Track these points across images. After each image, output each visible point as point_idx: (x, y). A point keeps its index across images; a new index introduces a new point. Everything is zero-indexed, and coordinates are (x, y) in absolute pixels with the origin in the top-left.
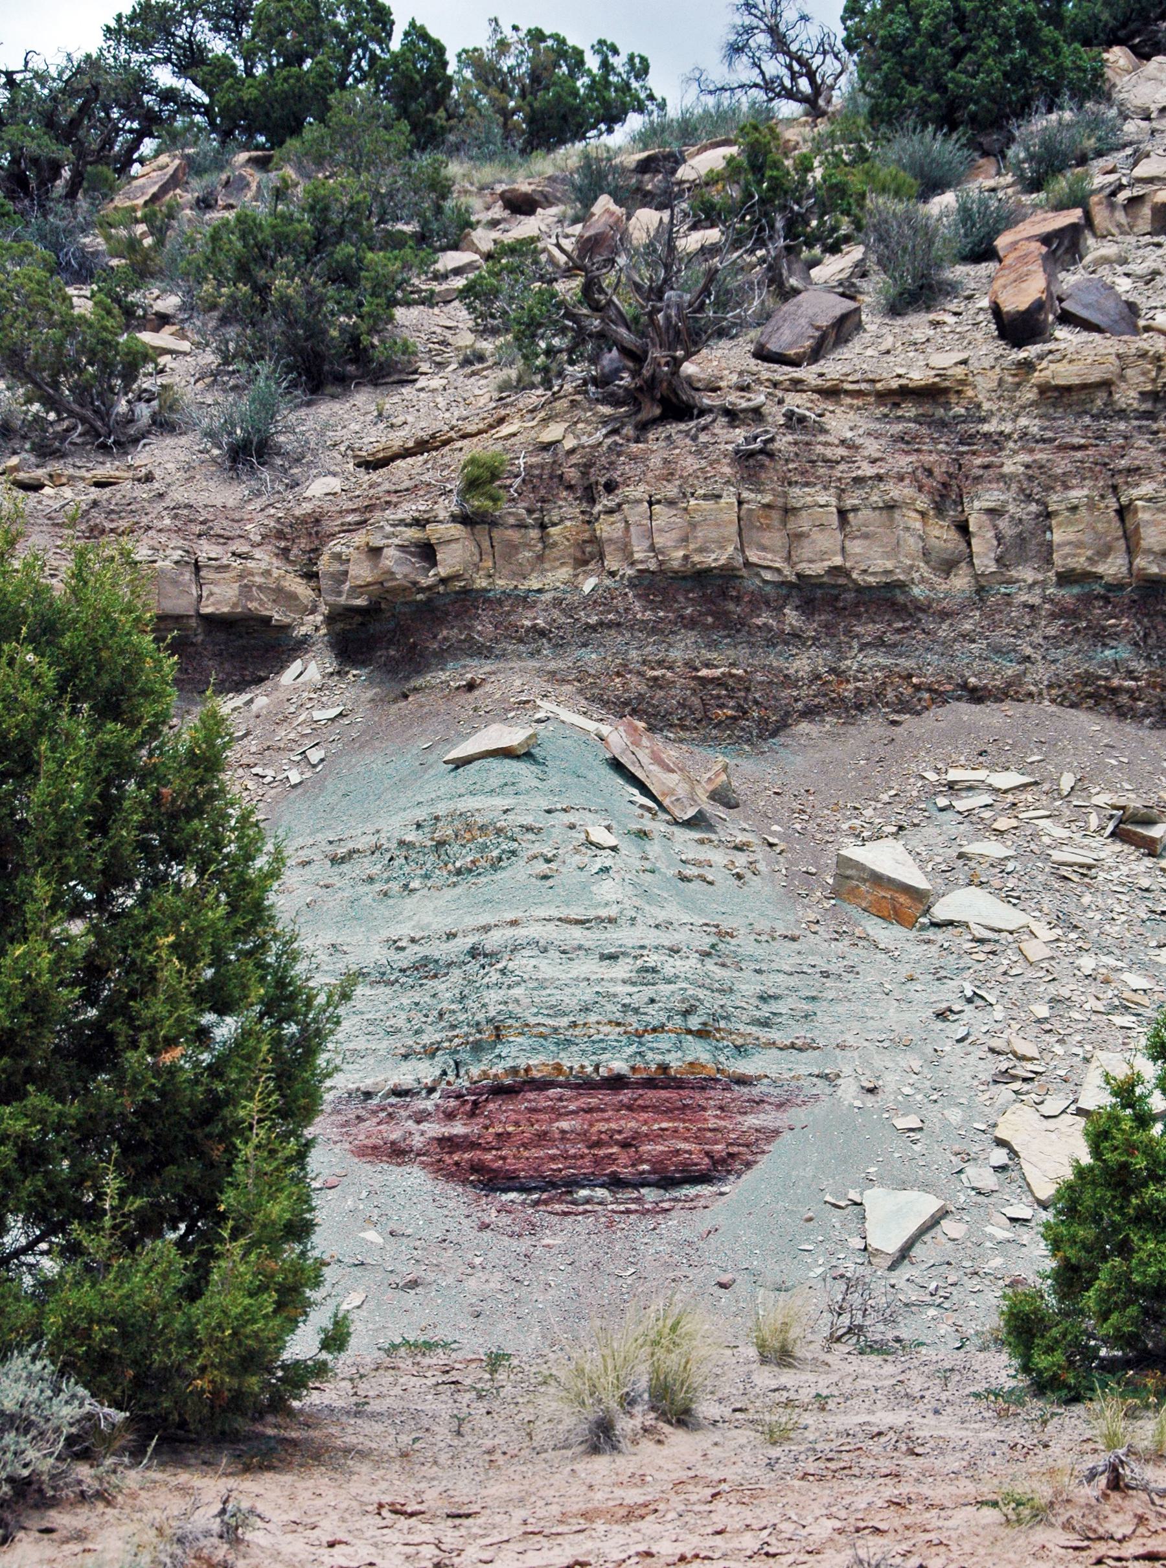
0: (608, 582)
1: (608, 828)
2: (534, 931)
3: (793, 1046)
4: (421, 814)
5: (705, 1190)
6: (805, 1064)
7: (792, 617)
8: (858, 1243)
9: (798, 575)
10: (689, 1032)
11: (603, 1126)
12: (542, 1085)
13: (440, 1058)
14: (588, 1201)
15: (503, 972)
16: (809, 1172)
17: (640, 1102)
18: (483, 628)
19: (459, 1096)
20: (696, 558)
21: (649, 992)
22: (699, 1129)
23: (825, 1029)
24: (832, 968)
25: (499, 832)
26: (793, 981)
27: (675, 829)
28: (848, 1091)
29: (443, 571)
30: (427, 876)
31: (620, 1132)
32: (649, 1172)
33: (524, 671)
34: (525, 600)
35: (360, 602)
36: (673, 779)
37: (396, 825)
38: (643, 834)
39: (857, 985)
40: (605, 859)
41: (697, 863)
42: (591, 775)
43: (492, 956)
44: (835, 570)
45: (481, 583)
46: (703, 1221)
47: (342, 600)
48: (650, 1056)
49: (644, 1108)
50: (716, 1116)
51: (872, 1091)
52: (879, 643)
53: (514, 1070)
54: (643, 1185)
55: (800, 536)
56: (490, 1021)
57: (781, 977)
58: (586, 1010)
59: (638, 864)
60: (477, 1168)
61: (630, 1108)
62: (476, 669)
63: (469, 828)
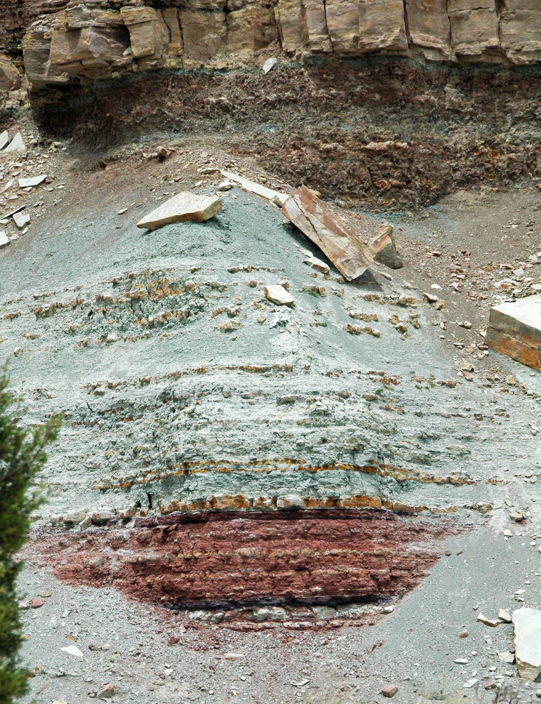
0: (286, 62)
1: (285, 286)
2: (219, 378)
3: (449, 481)
4: (118, 273)
5: (372, 609)
6: (460, 497)
7: (452, 94)
8: (507, 657)
9: (458, 55)
10: (357, 468)
11: (280, 552)
12: (227, 515)
13: (135, 491)
14: (266, 618)
15: (191, 414)
16: (464, 593)
17: (313, 530)
18: (173, 104)
19: (151, 525)
20: (365, 40)
21: (321, 432)
22: (366, 555)
23: (479, 466)
24: (485, 412)
25: (188, 289)
26: (450, 423)
27: (345, 287)
28: (499, 520)
29: (136, 51)
30: (123, 329)
31: (295, 557)
32: (321, 593)
33: (209, 143)
34: (210, 79)
35: (61, 79)
36: (343, 242)
37: (95, 282)
38: (316, 292)
39: (507, 427)
40: (282, 314)
41: (364, 318)
42: (270, 239)
43: (182, 401)
44: (491, 50)
45: (173, 63)
46: (369, 636)
47: (44, 77)
48: (322, 490)
49: (316, 536)
50: (381, 544)
51: (520, 521)
52: (531, 117)
53: (201, 502)
54: (316, 605)
55: (460, 19)
56: (179, 458)
57: (438, 420)
58: (265, 448)
59: (311, 319)
60: (167, 589)
61: (304, 536)
62: (167, 141)
63: (160, 286)
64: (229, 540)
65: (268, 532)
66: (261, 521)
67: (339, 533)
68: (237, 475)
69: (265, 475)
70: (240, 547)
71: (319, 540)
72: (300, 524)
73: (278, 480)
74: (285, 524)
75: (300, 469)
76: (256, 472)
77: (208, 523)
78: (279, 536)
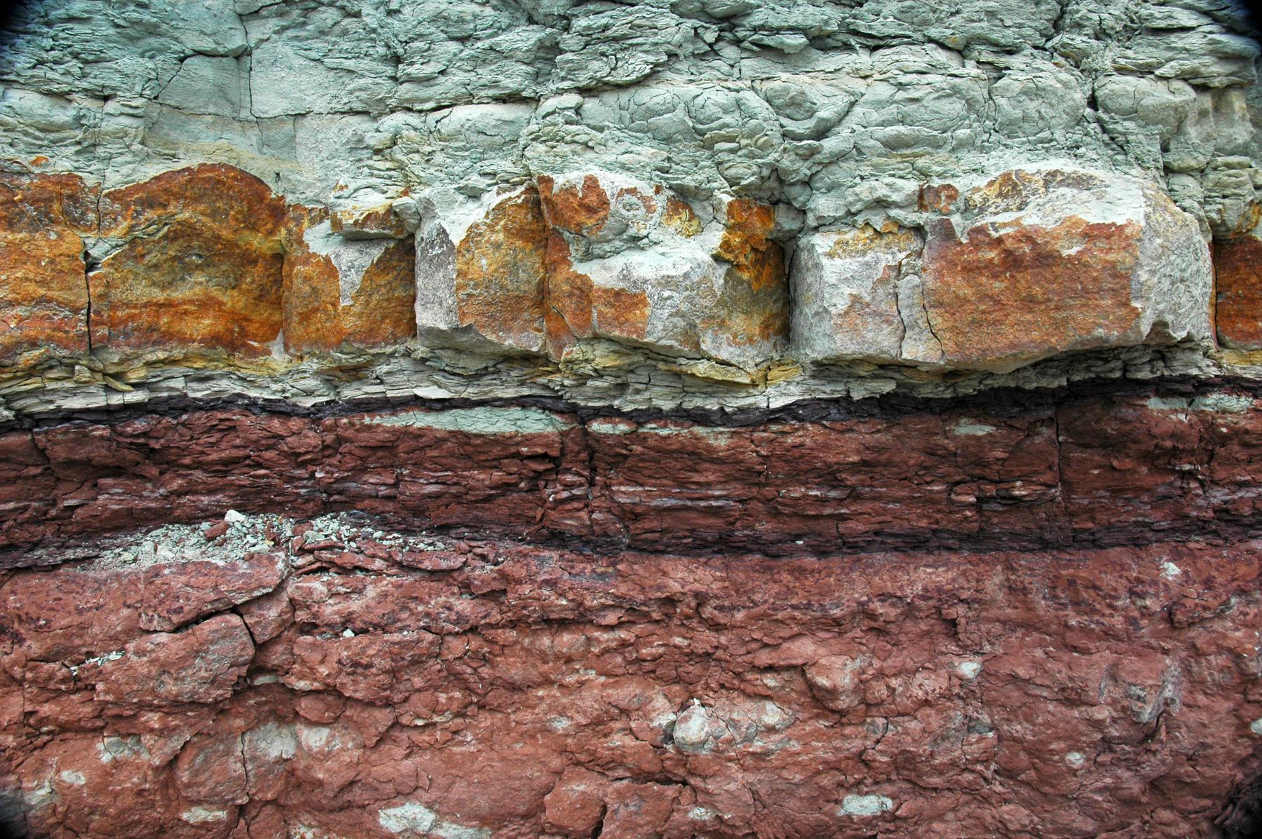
66: (548, 575)
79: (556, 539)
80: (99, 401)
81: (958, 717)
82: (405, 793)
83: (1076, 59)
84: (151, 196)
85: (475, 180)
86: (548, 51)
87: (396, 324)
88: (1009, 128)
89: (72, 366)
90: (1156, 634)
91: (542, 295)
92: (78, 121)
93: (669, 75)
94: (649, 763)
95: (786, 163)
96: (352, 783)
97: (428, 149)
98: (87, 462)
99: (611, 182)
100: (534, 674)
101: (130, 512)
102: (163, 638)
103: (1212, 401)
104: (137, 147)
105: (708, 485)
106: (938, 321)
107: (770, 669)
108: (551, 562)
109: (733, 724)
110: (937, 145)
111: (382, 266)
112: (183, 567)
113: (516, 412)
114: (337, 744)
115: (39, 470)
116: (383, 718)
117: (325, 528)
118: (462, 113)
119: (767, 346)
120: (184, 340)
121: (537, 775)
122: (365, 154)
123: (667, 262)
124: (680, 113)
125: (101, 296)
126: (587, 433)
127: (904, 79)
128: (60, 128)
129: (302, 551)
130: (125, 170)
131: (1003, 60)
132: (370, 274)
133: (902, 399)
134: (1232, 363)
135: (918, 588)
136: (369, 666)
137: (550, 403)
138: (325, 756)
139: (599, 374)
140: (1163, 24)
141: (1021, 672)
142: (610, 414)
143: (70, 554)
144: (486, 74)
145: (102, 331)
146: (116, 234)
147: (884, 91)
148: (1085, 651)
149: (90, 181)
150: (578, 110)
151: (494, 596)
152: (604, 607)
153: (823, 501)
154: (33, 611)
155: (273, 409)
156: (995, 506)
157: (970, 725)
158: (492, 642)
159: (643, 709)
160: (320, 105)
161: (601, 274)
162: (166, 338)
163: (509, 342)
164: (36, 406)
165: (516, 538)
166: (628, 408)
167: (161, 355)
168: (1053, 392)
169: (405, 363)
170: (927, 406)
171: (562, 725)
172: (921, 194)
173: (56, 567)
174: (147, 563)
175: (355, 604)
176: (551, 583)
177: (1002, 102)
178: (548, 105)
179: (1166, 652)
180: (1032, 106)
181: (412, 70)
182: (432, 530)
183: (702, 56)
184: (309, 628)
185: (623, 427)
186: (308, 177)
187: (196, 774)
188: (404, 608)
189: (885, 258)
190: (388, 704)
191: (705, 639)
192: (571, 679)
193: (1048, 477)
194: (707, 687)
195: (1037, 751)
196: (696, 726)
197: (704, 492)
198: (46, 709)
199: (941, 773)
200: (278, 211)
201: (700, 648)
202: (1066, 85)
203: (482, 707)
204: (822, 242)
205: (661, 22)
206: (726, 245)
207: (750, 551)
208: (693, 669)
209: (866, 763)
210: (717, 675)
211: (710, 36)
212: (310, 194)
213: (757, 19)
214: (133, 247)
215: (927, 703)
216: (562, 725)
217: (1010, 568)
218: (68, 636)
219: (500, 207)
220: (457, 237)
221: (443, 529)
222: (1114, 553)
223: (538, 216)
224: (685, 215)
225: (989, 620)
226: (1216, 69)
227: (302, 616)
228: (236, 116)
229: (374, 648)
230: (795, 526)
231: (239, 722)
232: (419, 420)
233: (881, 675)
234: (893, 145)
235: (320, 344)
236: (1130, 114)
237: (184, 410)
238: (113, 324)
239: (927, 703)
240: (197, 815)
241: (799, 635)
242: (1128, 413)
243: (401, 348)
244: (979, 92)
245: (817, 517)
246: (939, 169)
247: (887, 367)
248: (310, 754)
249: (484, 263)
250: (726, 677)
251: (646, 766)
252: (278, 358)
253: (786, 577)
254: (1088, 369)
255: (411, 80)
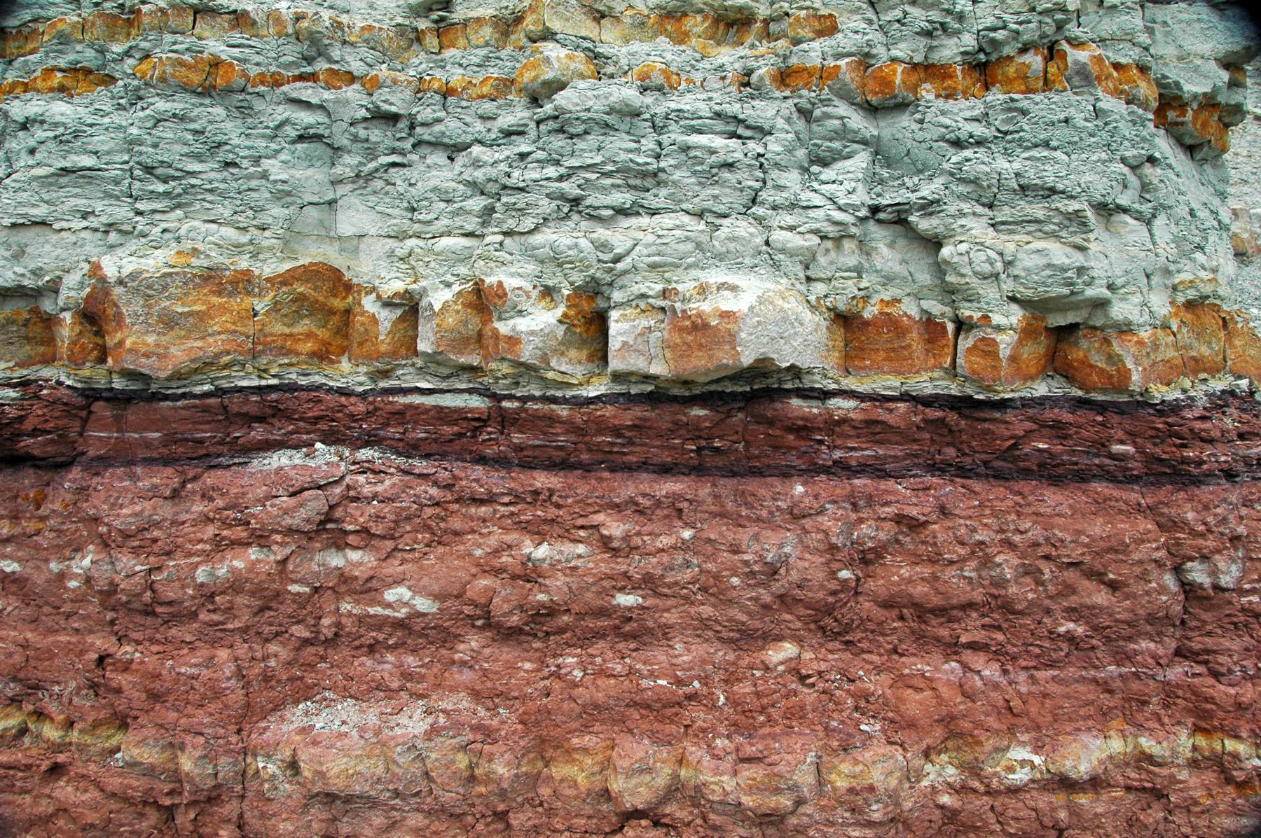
17: (901, 573)
48: (973, 241)
49: (927, 620)
64: (216, 636)
65: (530, 574)
66: (477, 478)
67: (1101, 597)
68: (306, 118)
69: (517, 114)
70: (304, 693)
71: (952, 649)
72: (796, 515)
73: (619, 146)
74: (676, 511)
75: (784, 77)
76: (447, 93)
77: (76, 473)
78: (626, 616)
79: (482, 460)
80: (256, 382)
81: (680, 560)
82: (398, 582)
83: (759, 220)
84: (285, 280)
85: (451, 279)
86: (490, 210)
87: (408, 349)
88: (720, 257)
89: (244, 365)
90: (784, 521)
91: (480, 335)
92: (251, 242)
93: (544, 229)
94: (518, 570)
95: (598, 275)
96: (372, 577)
97: (427, 259)
98: (246, 415)
99: (510, 283)
100: (467, 527)
101: (267, 440)
102: (285, 499)
103: (835, 402)
104: (279, 254)
105: (557, 434)
106: (668, 355)
107: (582, 527)
108: (479, 471)
109: (561, 552)
110: (677, 267)
111: (402, 319)
112: (295, 467)
113: (466, 396)
114: (366, 559)
115: (221, 417)
116: (389, 545)
117: (365, 454)
118: (446, 242)
119: (591, 366)
120: (298, 354)
121: (464, 576)
122: (396, 259)
123: (534, 323)
124: (547, 249)
125: (260, 330)
126: (501, 408)
127: (660, 233)
128: (243, 245)
129: (354, 463)
130: (273, 266)
131: (718, 222)
132: (395, 324)
133: (659, 395)
134: (850, 383)
135: (664, 492)
136: (384, 518)
137: (484, 392)
138: (361, 564)
139: (505, 377)
140: (805, 204)
141: (712, 537)
142: (511, 397)
143: (236, 460)
144: (458, 221)
145: (260, 348)
146: (268, 299)
147: (650, 238)
148: (744, 527)
149: (257, 272)
150: (501, 244)
151: (449, 487)
152: (503, 494)
153: (613, 444)
154: (220, 486)
155: (341, 392)
156: (706, 452)
157: (688, 564)
158: (446, 510)
159: (518, 545)
160: (373, 231)
161: (503, 328)
162: (290, 352)
163: (462, 360)
164: (225, 384)
165: (464, 461)
166: (519, 395)
167: (287, 361)
168: (743, 394)
169: (411, 370)
170: (675, 399)
171: (478, 552)
172: (664, 291)
173: (229, 466)
174: (275, 465)
175: (379, 488)
176: (477, 481)
177: (716, 243)
178: (488, 239)
179: (789, 530)
180: (732, 246)
181: (420, 217)
182: (421, 457)
183: (562, 219)
184: (356, 499)
185: (516, 404)
186: (365, 270)
187: (296, 567)
188: (404, 492)
189: (644, 322)
190: (393, 538)
191: (552, 512)
192: (484, 531)
193: (734, 438)
194: (552, 536)
195: (717, 577)
196: (542, 552)
197: (555, 438)
198: (225, 533)
199: (670, 588)
200: (348, 287)
201: (549, 516)
202: (751, 234)
203: (439, 543)
204: (614, 315)
205: (541, 203)
206: (565, 315)
207: (576, 469)
208: (546, 528)
209: (629, 578)
210: (557, 530)
211: (566, 210)
212: (366, 279)
213: (588, 202)
214: (276, 307)
215: (663, 550)
216: (478, 552)
217: (714, 485)
218: (236, 498)
219: (460, 292)
220: (437, 308)
221: (427, 456)
222: (769, 479)
223: (479, 297)
224: (548, 299)
225: (702, 512)
226: (830, 229)
227: (352, 493)
228: (329, 235)
229: (387, 509)
230: (600, 457)
231: (318, 545)
232: (417, 399)
233: (639, 534)
234: (653, 266)
235: (369, 358)
236: (782, 251)
237: (296, 390)
238: (265, 344)
239: (663, 550)
240: (295, 588)
241: (598, 512)
242: (778, 405)
243: (410, 362)
244: (704, 238)
245: (611, 452)
246: (675, 278)
247: (647, 378)
248: (352, 564)
249: (450, 321)
250: (561, 531)
251: (517, 572)
252: (345, 365)
253: (593, 482)
254: (761, 382)
255: (419, 222)
